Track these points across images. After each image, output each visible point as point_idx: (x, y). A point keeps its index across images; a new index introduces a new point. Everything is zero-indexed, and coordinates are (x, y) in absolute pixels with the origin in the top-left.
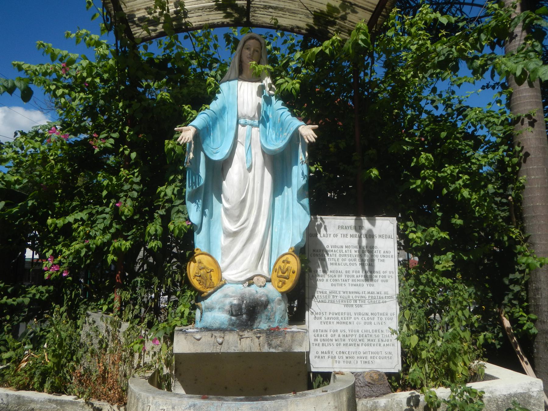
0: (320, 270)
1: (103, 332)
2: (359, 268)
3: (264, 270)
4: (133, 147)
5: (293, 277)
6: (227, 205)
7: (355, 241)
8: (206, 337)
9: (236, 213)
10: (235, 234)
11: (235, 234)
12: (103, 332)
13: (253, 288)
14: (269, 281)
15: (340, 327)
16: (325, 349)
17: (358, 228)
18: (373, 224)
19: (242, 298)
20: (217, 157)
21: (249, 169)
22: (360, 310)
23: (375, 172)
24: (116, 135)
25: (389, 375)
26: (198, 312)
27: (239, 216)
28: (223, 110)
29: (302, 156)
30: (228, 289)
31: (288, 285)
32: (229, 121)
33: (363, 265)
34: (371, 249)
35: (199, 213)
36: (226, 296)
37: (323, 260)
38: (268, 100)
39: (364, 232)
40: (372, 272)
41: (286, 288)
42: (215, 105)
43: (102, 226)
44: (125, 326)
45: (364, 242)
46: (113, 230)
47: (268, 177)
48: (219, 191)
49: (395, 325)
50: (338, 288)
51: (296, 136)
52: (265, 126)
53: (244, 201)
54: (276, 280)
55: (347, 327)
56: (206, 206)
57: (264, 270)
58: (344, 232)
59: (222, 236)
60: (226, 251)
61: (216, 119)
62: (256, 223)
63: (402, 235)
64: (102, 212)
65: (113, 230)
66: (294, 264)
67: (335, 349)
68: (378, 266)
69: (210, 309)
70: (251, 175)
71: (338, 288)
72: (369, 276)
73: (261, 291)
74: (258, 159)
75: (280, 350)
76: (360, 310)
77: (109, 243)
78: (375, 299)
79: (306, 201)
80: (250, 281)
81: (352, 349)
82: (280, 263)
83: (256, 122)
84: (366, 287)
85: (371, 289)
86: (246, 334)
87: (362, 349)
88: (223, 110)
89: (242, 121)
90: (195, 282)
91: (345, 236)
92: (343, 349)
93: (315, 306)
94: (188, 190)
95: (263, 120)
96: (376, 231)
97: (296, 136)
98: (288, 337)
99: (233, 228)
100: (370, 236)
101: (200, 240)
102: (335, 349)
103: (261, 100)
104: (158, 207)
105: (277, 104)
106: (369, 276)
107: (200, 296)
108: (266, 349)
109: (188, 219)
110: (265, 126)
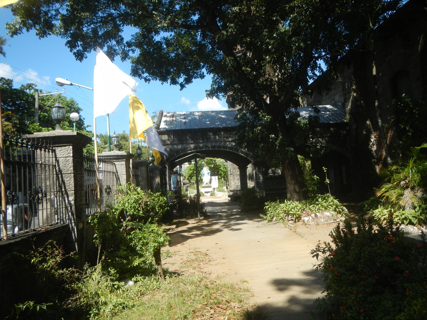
63: (218, 177)
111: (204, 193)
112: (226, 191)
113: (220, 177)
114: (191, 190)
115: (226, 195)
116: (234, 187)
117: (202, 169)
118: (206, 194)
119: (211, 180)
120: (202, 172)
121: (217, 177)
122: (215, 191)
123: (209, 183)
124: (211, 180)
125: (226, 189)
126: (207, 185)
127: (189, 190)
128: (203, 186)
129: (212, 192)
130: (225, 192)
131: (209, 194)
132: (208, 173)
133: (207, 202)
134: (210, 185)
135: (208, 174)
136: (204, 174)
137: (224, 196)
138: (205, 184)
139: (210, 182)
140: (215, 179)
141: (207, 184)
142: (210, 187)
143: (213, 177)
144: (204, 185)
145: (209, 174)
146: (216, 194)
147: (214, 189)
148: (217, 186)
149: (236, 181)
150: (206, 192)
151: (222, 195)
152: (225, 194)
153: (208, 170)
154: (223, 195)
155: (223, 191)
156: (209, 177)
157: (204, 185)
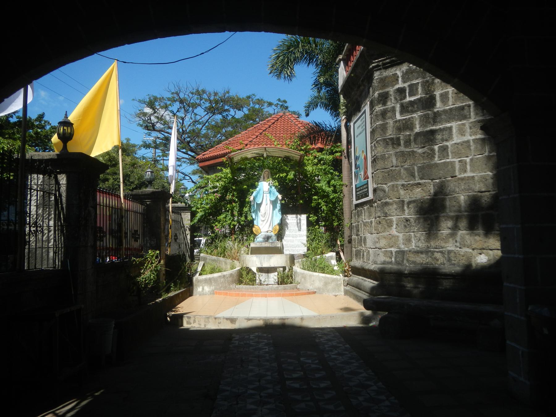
0: (286, 229)
1: (231, 246)
2: (297, 228)
3: (271, 229)
4: (236, 198)
5: (277, 231)
6: (262, 214)
7: (296, 221)
8: (258, 244)
9: (264, 216)
10: (263, 221)
11: (263, 221)
12: (231, 246)
13: (268, 233)
14: (272, 232)
15: (291, 243)
16: (288, 248)
17: (297, 218)
18: (301, 216)
19: (265, 236)
20: (259, 202)
21: (267, 205)
22: (297, 239)
23: (301, 201)
24: (231, 194)
25: (304, 255)
26: (255, 239)
27: (264, 217)
28: (260, 190)
29: (279, 202)
30: (262, 233)
31: (276, 232)
32: (261, 192)
33: (298, 227)
34: (300, 223)
35: (255, 216)
36: (262, 235)
37: (287, 226)
38: (271, 187)
39: (298, 219)
40: (301, 229)
41: (276, 233)
42: (257, 189)
43: (229, 218)
44: (236, 244)
45: (298, 221)
46: (231, 219)
47: (271, 206)
48: (260, 210)
49: (305, 242)
50: (290, 233)
51: (277, 197)
52: (270, 194)
53: (265, 213)
54: (273, 231)
55: (293, 243)
56: (256, 214)
57: (271, 229)
58: (292, 219)
59: (260, 221)
60: (262, 224)
61: (258, 193)
62: (268, 218)
63: (308, 218)
64: (228, 214)
65: (231, 219)
66: (278, 227)
67: (290, 249)
68: (302, 228)
69: (258, 238)
70: (267, 206)
71: (290, 233)
72: (300, 230)
73: (270, 234)
74: (269, 202)
75: (274, 246)
76: (296, 239)
77: (231, 223)
78: (301, 236)
79: (280, 212)
80: (267, 232)
81: (294, 248)
82: (275, 227)
83: (268, 193)
84: (298, 233)
85: (299, 233)
86: (267, 243)
87: (297, 248)
88: (260, 190)
89: (264, 192)
90: (255, 232)
91: (292, 220)
92: (292, 248)
93: (285, 238)
94: (252, 211)
95: (270, 192)
96: (301, 219)
97: (277, 197)
98: (276, 243)
99: (263, 219)
100: (300, 220)
101: (255, 222)
102: (290, 249)
103: (269, 187)
104: (243, 213)
105: (273, 188)
106: (300, 230)
107: (256, 235)
108: (271, 246)
109: (252, 217)
110: (270, 194)
111: (254, 270)
112: (336, 268)
113: (313, 218)
114: (209, 257)
115: (338, 286)
116: (382, 258)
117: (254, 187)
118: (262, 277)
119: (282, 226)
120: (252, 198)
121: (304, 217)
122: (297, 268)
123: (274, 238)
124: (282, 226)
125: (334, 262)
126: (267, 245)
127: (205, 259)
128: (252, 245)
129: (284, 268)
130: (332, 272)
131: (273, 277)
132: (274, 203)
133: (261, 323)
134: (279, 244)
135: (274, 207)
136: (259, 205)
137: (330, 287)
138: (260, 238)
139: (280, 236)
140: (299, 224)
141: (267, 238)
142: (279, 251)
143: (291, 219)
144: (258, 242)
145: (279, 206)
146: (298, 279)
147: (292, 258)
148: (303, 250)
149: (394, 231)
150: (261, 270)
151: (318, 284)
152: (334, 280)
153: (274, 189)
154: (326, 284)
155: (324, 269)
156: (278, 217)
157: (258, 242)
